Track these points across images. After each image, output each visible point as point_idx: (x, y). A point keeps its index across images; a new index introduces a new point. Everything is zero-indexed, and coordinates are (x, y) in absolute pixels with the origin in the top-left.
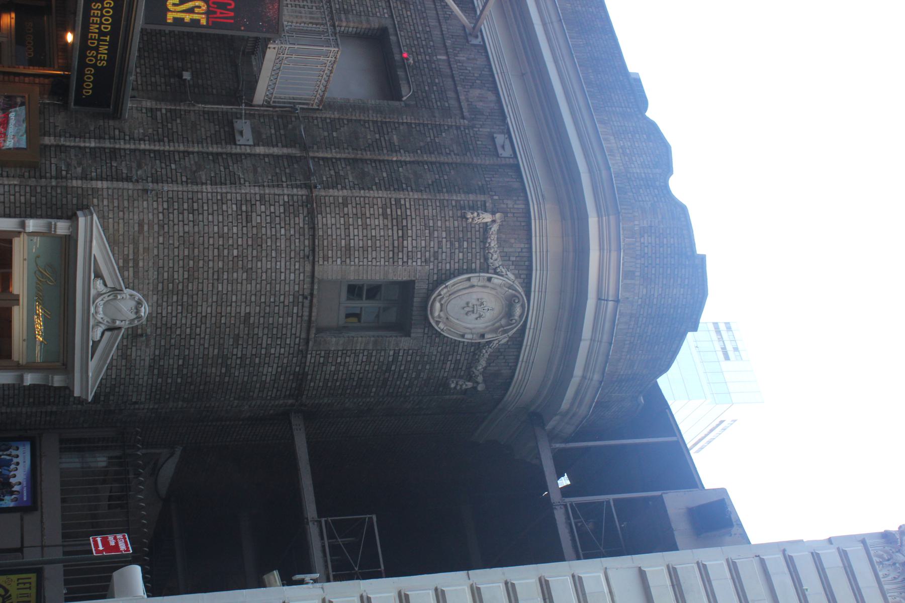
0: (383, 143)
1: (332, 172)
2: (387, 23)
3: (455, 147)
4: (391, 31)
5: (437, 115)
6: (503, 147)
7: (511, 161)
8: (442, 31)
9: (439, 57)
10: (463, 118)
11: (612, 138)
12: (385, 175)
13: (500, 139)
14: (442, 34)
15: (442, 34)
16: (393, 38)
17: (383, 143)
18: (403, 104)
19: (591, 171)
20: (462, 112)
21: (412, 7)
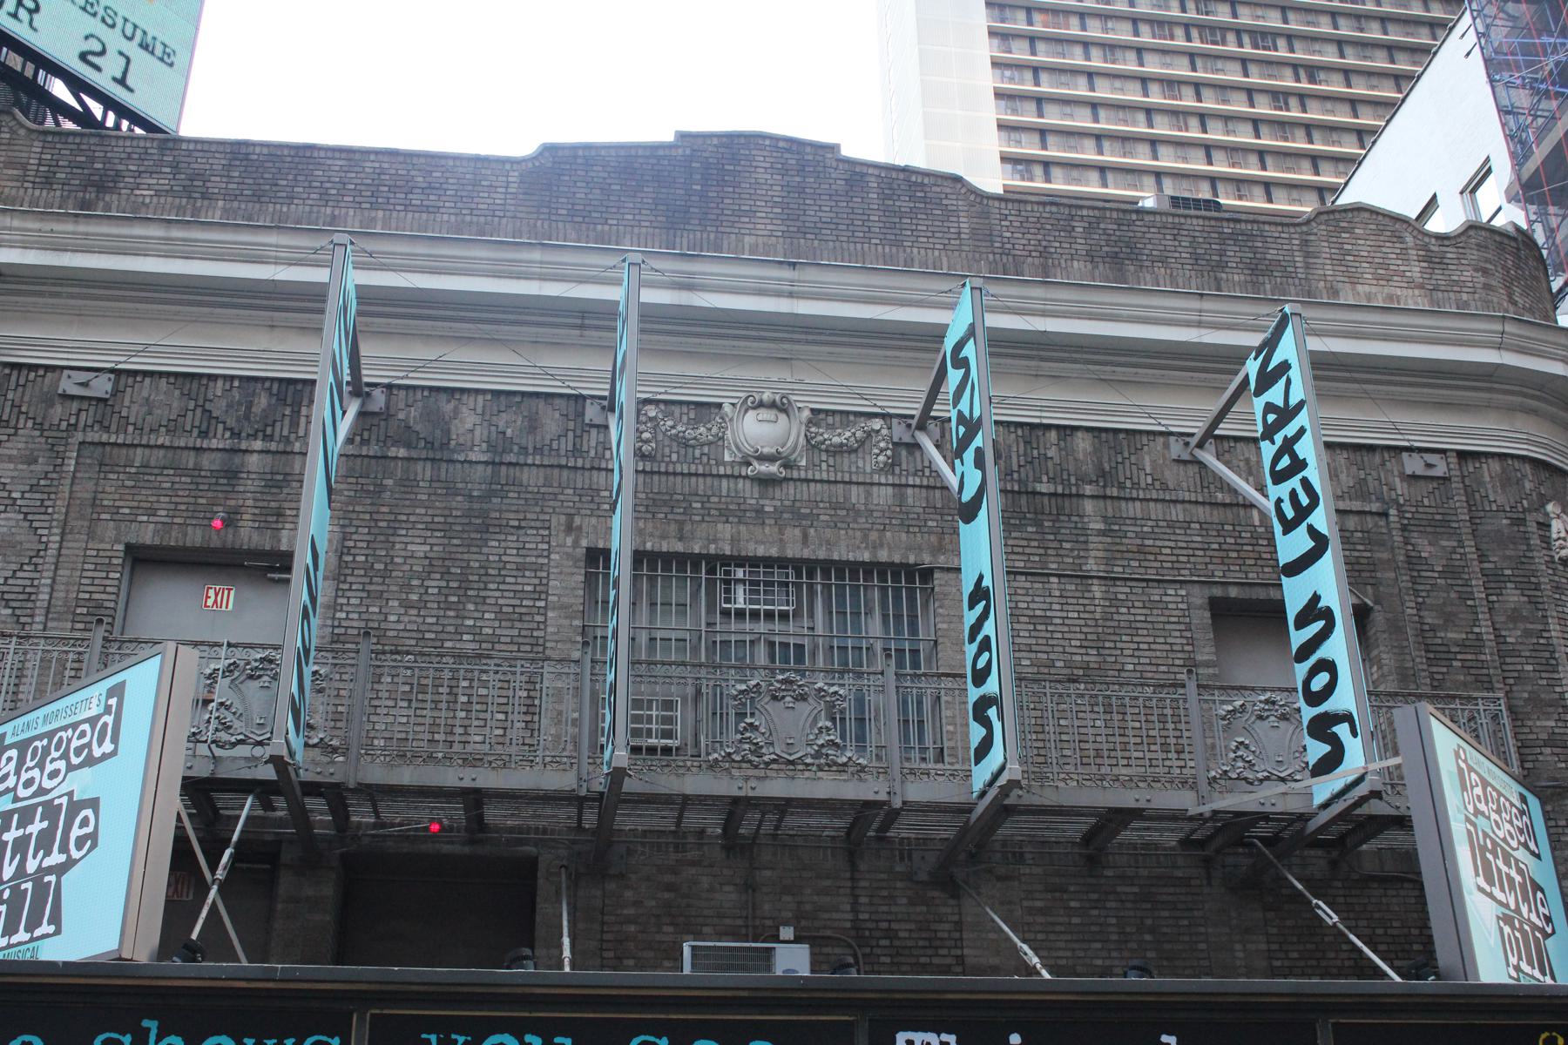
0: (1469, 657)
1: (1548, 751)
2: (1199, 597)
3: (1444, 543)
4: (1217, 592)
5: (1385, 556)
6: (1429, 466)
7: (1453, 460)
8: (1196, 502)
9: (1257, 523)
10: (1385, 515)
11: (1359, 287)
12: (1530, 668)
13: (1413, 465)
14: (1203, 503)
15: (1203, 503)
16: (1233, 592)
17: (1469, 657)
18: (1377, 607)
19: (1499, 347)
20: (1370, 513)
21: (1147, 542)
